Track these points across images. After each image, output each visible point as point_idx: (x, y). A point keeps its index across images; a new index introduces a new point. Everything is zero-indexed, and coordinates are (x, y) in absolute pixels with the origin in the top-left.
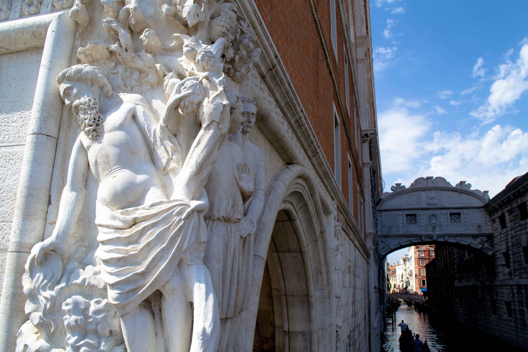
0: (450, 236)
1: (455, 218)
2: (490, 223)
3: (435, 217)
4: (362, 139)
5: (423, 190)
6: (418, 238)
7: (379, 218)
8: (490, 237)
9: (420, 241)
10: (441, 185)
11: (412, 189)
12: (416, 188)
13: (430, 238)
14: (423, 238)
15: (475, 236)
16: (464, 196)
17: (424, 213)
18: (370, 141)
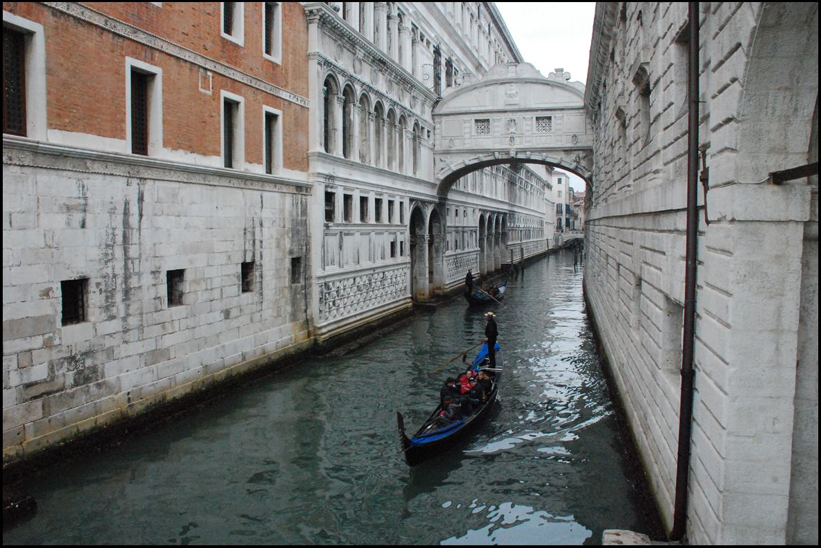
0: (534, 150)
1: (544, 124)
2: (590, 132)
3: (515, 124)
4: (308, 18)
5: (502, 84)
6: (490, 154)
7: (438, 126)
8: (589, 151)
9: (491, 158)
10: (526, 76)
11: (484, 83)
12: (491, 81)
13: (506, 154)
14: (497, 154)
15: (567, 151)
16: (558, 91)
17: (499, 118)
18: (319, 20)
